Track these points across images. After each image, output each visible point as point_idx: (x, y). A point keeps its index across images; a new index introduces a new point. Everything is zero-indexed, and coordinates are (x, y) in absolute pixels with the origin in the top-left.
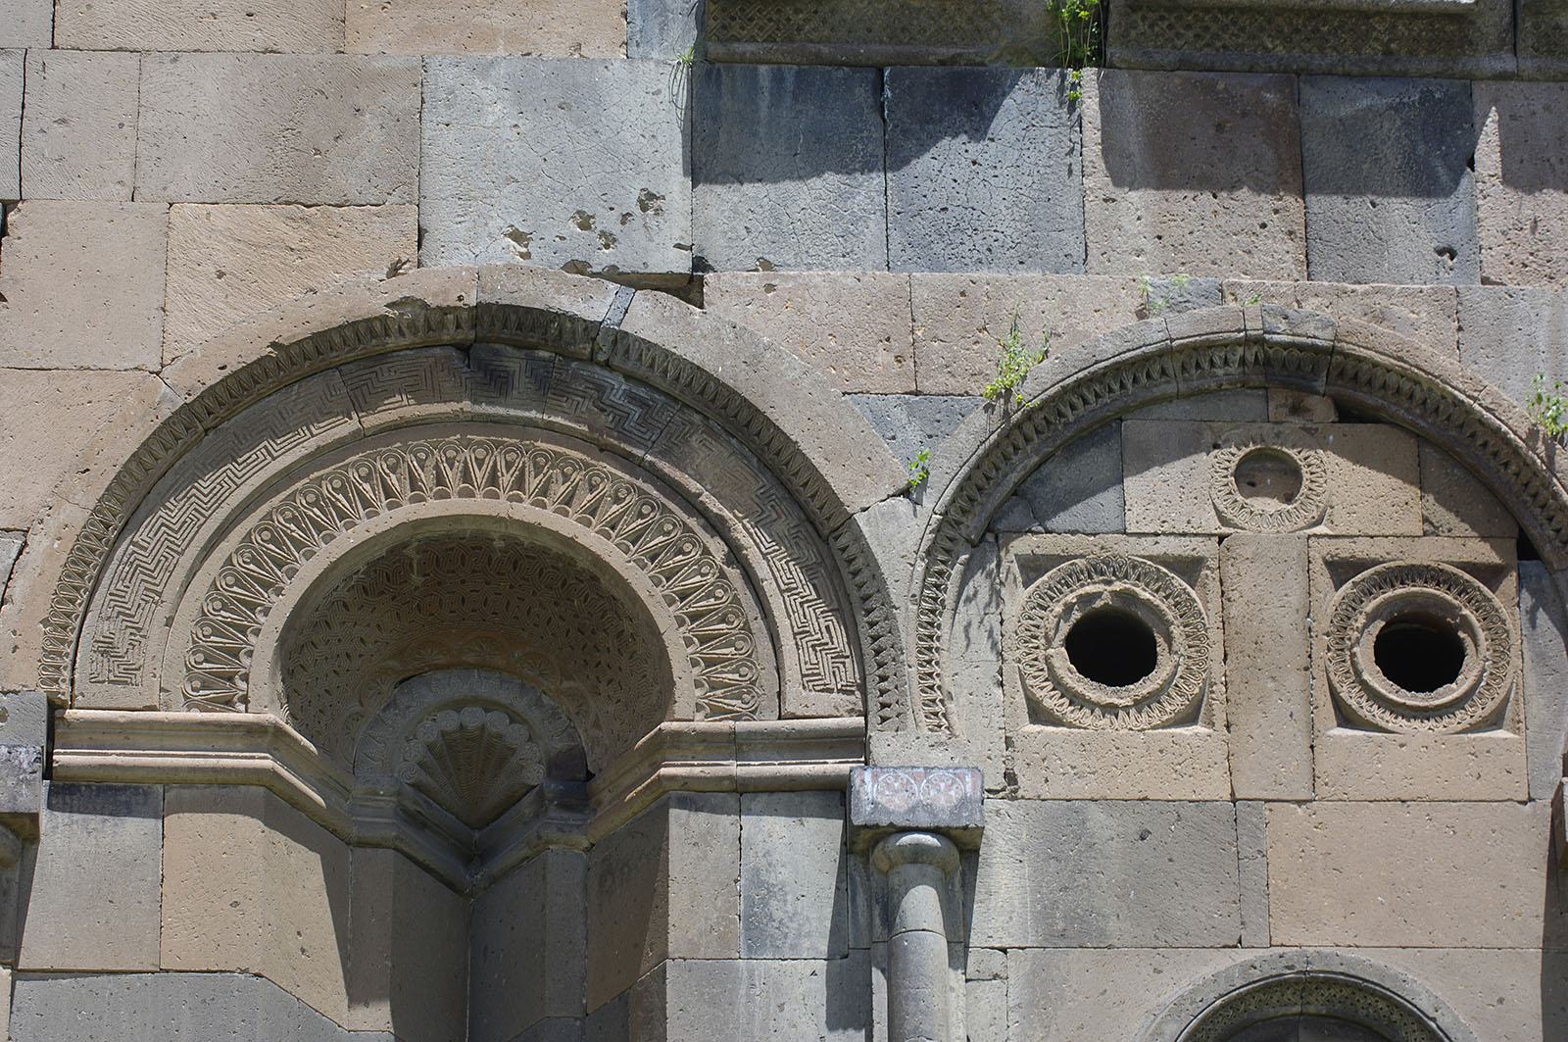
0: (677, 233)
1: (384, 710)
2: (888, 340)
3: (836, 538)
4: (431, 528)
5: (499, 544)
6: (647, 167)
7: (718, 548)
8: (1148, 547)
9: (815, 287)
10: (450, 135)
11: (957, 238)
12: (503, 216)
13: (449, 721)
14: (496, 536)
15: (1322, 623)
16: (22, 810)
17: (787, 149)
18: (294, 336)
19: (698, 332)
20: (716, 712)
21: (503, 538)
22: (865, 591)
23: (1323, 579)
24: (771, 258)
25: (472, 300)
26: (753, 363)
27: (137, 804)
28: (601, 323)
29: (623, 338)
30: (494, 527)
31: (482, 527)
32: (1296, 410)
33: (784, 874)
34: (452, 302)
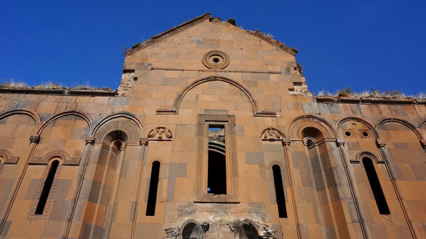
7: (325, 129)
8: (349, 128)
10: (304, 107)
15: (360, 133)
20: (326, 137)
23: (359, 130)
25: (308, 115)
26: (325, 118)
32: (354, 121)
33: (333, 146)
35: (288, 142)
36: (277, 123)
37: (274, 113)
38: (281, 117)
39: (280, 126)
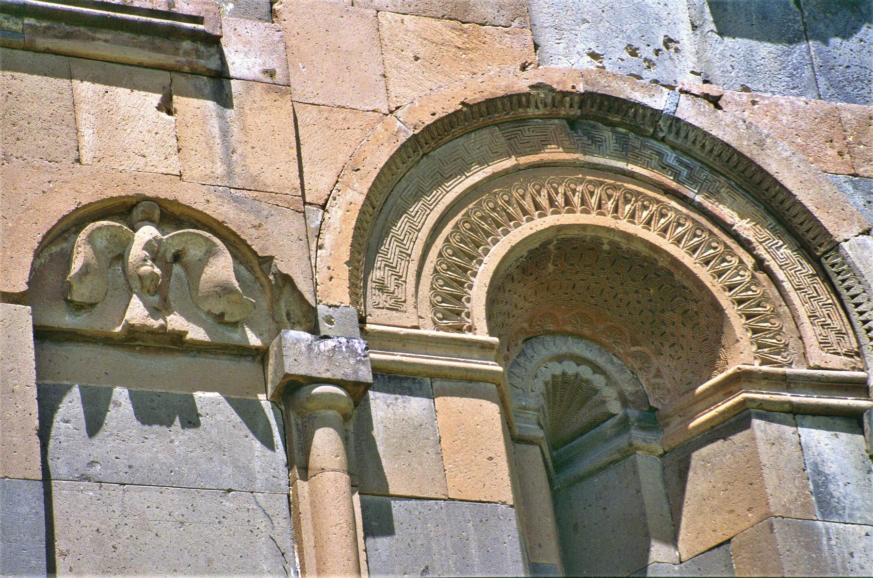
0: (691, 65)
1: (518, 357)
2: (831, 141)
3: (826, 259)
4: (567, 232)
5: (606, 247)
6: (665, 23)
7: (749, 261)
9: (782, 105)
11: (859, 84)
12: (584, 42)
13: (557, 369)
14: (605, 241)
16: (362, 380)
17: (746, 21)
18: (475, 99)
19: (723, 122)
20: (764, 362)
21: (611, 243)
22: (852, 292)
24: (749, 85)
25: (581, 88)
27: (416, 389)
28: (662, 111)
29: (677, 122)
30: (606, 235)
31: (599, 235)
34: (569, 88)
35: (339, 376)
36: (229, 151)
37: (200, 27)
38: (279, 78)
39: (257, 188)
